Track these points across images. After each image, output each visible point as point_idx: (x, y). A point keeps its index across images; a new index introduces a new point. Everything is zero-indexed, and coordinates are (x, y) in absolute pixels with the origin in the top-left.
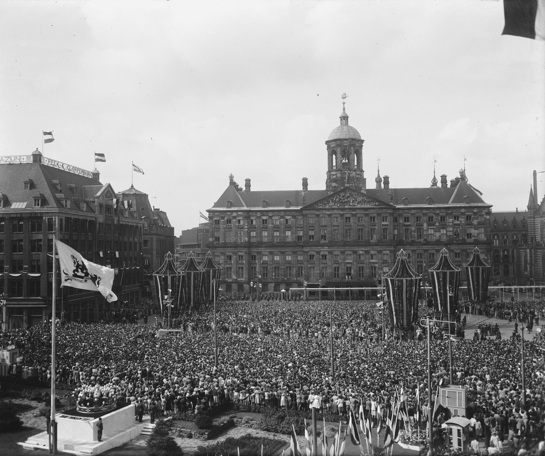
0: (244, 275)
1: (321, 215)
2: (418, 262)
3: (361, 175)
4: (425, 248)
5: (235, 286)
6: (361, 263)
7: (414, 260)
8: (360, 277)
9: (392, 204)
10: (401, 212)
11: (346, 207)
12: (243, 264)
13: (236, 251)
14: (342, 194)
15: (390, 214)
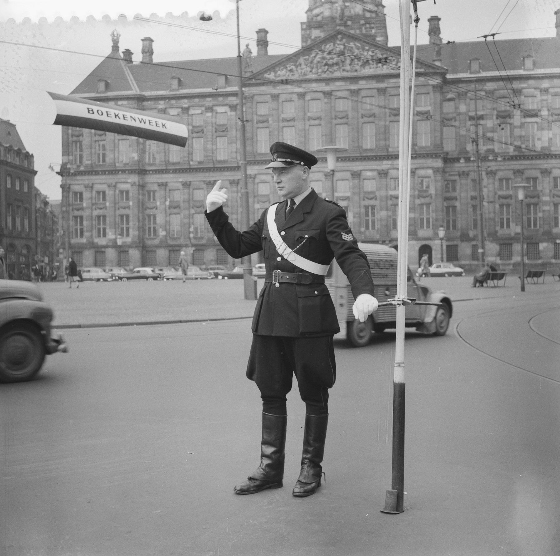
0: (131, 230)
1: (283, 97)
2: (501, 197)
3: (377, 14)
4: (517, 167)
5: (111, 253)
6: (371, 199)
7: (491, 194)
8: (367, 228)
9: (438, 64)
10: (463, 87)
11: (337, 74)
12: (128, 207)
13: (116, 180)
14: (329, 47)
15: (434, 86)
